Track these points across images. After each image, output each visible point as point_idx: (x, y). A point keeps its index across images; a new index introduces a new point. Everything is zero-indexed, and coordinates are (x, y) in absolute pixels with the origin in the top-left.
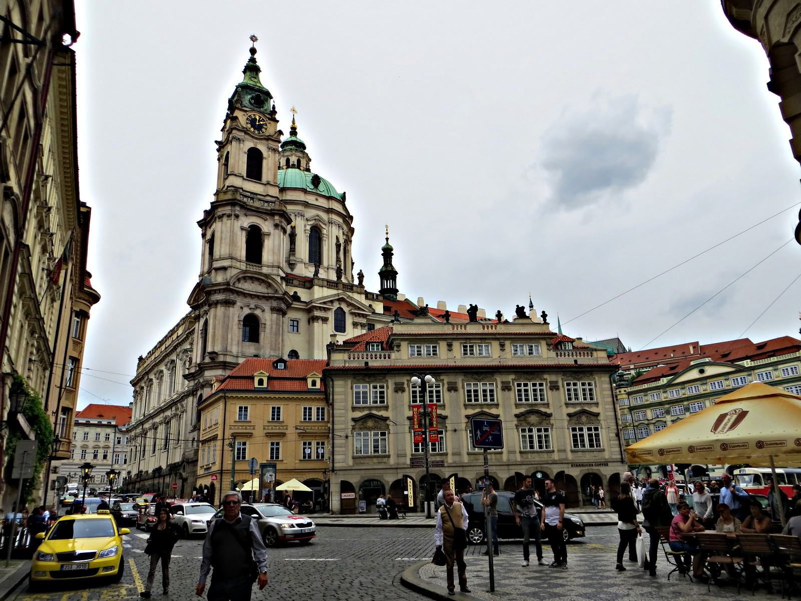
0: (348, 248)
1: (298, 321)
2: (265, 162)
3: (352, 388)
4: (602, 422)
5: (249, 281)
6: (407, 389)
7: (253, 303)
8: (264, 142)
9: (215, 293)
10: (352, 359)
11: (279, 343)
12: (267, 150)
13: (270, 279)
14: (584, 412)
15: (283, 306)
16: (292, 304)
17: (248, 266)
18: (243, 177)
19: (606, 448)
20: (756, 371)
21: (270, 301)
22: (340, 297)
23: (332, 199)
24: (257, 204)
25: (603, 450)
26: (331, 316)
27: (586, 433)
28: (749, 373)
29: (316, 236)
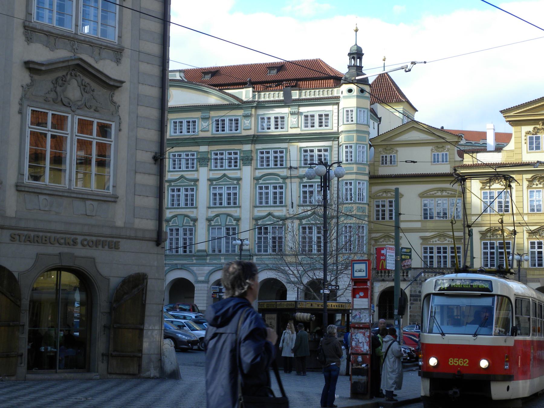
4: (124, 112)
14: (81, 68)
19: (121, 192)
20: (261, 112)
25: (114, 199)
27: (71, 132)
28: (248, 112)
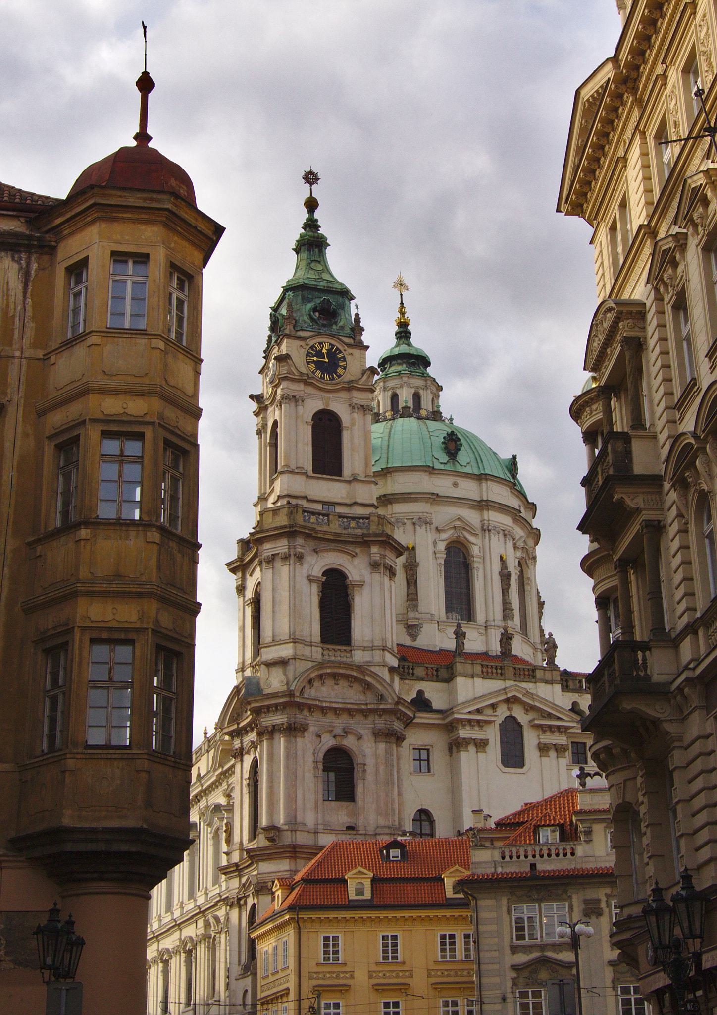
0: (528, 573)
1: (428, 750)
2: (346, 435)
3: (509, 912)
5: (330, 682)
6: (606, 910)
7: (339, 723)
8: (343, 395)
9: (269, 711)
10: (507, 859)
11: (393, 801)
12: (349, 410)
13: (368, 674)
15: (397, 725)
16: (415, 717)
17: (326, 652)
18: (306, 474)
21: (371, 718)
22: (509, 695)
23: (487, 480)
24: (335, 527)
26: (493, 734)
29: (458, 564)
